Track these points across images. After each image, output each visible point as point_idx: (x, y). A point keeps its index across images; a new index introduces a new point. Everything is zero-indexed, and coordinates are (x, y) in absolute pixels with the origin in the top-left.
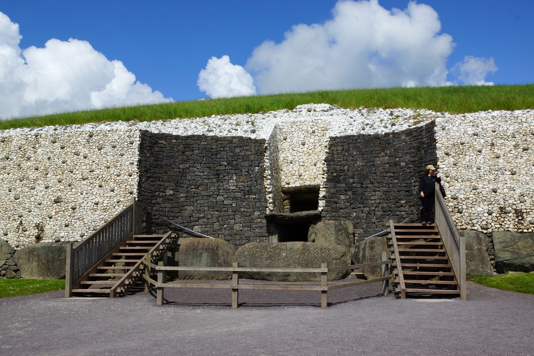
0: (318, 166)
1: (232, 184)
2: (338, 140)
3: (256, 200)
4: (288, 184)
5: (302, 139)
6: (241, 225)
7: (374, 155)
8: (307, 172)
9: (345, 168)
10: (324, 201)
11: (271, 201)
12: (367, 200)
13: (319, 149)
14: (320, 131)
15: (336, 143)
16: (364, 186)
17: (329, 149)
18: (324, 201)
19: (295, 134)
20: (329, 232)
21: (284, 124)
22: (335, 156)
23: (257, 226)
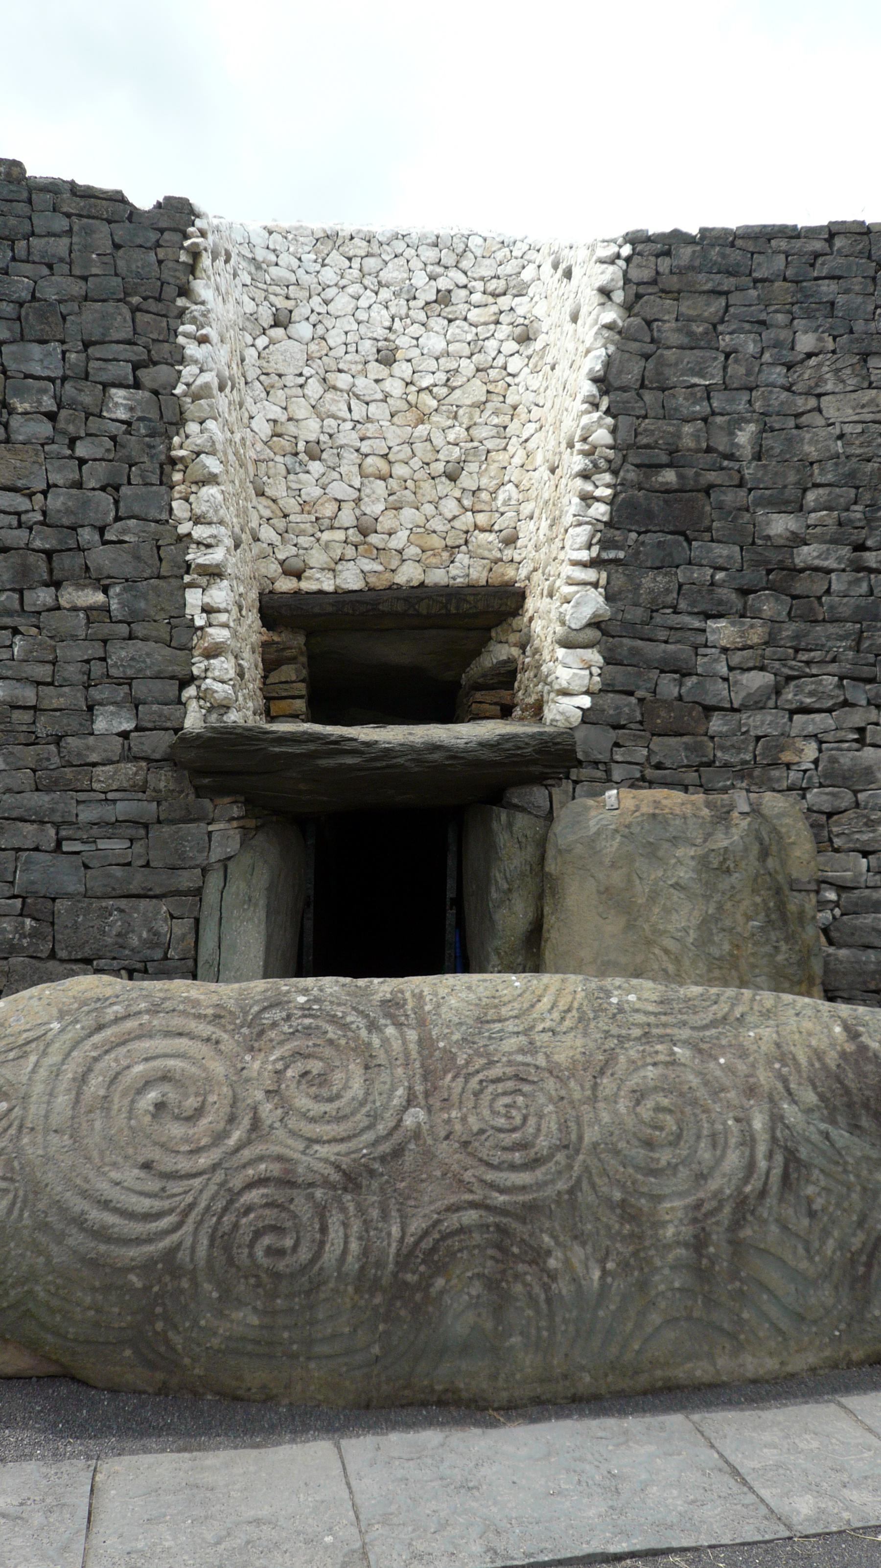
0: (466, 481)
3: (106, 629)
4: (298, 575)
5: (380, 333)
8: (408, 514)
11: (218, 634)
13: (477, 390)
14: (477, 298)
15: (678, 272)
17: (628, 308)
18: (594, 656)
19: (342, 303)
21: (276, 241)
22: (670, 355)
23: (110, 813)
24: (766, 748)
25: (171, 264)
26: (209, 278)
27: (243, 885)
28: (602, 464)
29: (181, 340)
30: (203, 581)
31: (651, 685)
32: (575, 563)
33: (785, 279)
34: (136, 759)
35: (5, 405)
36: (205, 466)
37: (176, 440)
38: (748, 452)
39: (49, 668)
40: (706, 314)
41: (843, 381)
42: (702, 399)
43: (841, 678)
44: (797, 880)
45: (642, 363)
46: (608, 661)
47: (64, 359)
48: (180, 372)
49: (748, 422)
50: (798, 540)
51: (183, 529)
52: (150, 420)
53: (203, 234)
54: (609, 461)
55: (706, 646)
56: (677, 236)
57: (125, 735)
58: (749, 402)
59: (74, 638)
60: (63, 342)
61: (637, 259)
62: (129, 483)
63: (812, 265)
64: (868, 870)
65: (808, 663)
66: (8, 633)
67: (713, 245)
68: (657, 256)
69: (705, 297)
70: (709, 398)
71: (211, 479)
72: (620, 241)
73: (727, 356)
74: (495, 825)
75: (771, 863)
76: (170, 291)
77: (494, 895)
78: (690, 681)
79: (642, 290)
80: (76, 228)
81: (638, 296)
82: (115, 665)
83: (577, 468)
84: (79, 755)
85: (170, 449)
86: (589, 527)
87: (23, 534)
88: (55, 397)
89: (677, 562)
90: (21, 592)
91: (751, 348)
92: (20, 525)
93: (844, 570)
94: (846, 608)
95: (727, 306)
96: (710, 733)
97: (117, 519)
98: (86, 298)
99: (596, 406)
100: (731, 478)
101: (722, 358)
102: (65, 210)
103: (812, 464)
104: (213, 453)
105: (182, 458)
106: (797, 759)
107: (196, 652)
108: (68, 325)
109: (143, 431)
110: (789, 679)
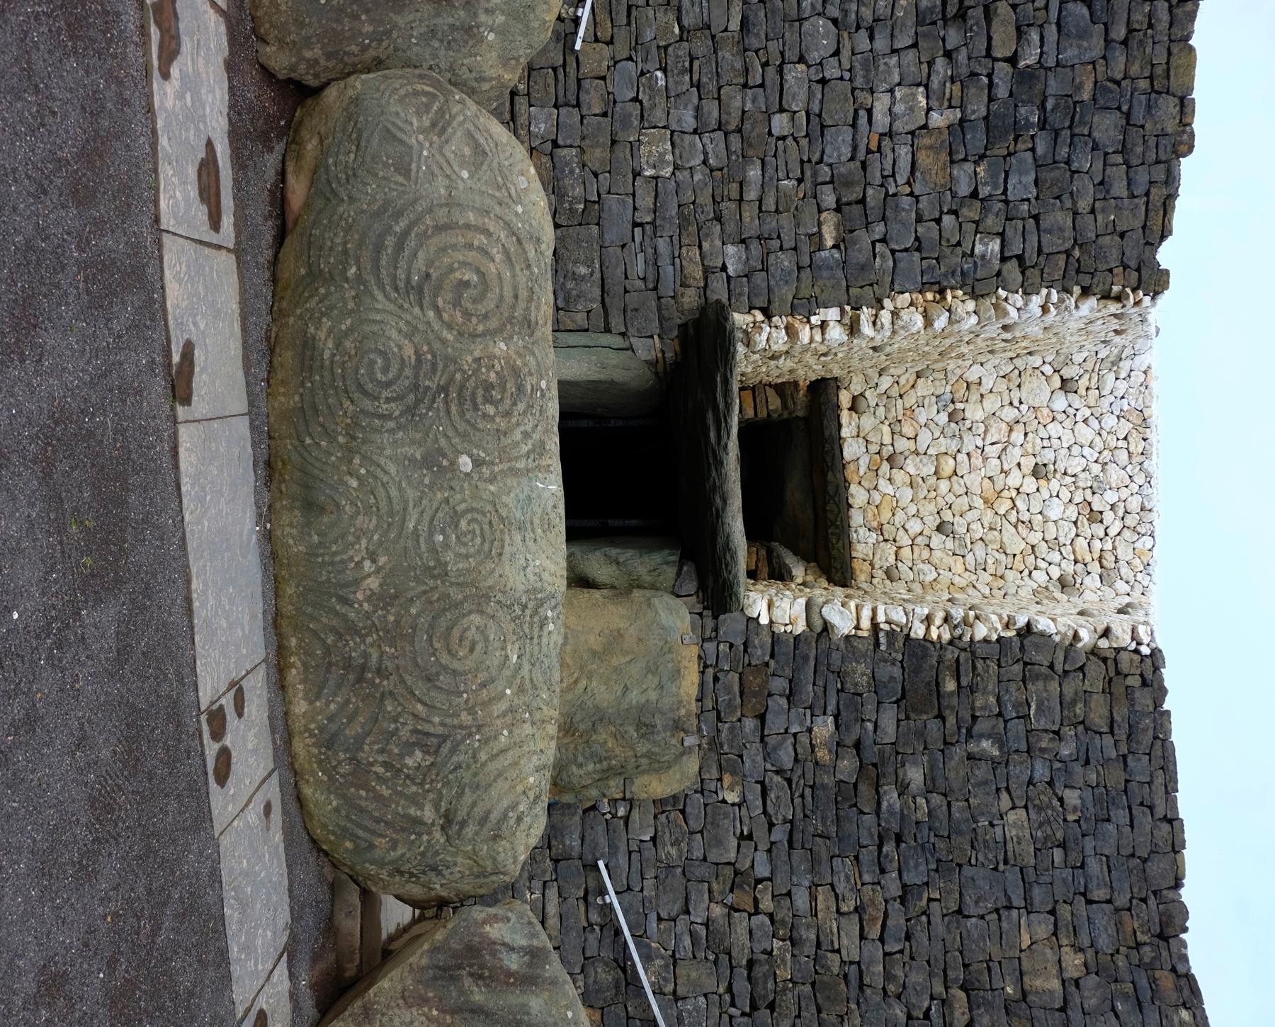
1: (897, 104)
2: (1144, 699)
3: (805, 248)
6: (667, 172)
7: (1064, 911)
9: (985, 744)
10: (800, 627)
11: (805, 334)
12: (812, 870)
14: (1097, 545)
16: (889, 848)
17: (1094, 652)
18: (800, 627)
20: (635, 670)
22: (1054, 686)
23: (665, 261)
24: (736, 761)
25: (1109, 280)
26: (1099, 311)
27: (614, 362)
28: (958, 632)
29: (1044, 291)
30: (847, 320)
31: (779, 673)
32: (874, 611)
33: (1127, 781)
34: (706, 279)
35: (982, 157)
36: (939, 317)
37: (960, 293)
38: (972, 747)
39: (773, 208)
40: (1092, 716)
41: (1040, 827)
42: (1017, 712)
43: (791, 822)
44: (632, 783)
45: (1046, 663)
46: (797, 638)
47: (1023, 200)
48: (1017, 292)
49: (1000, 750)
50: (903, 788)
51: (887, 302)
52: (975, 272)
53: (1137, 303)
54: (960, 638)
55: (812, 715)
56: (1163, 691)
57: (724, 268)
58: (1017, 751)
59: (797, 225)
60: (1037, 199)
61: (1136, 657)
62: (922, 259)
63: (1142, 804)
64: (641, 841)
65: (802, 796)
66: (799, 174)
67: (1154, 721)
68: (1141, 675)
69: (1108, 714)
70: (1018, 717)
71: (928, 323)
72: (1153, 645)
73: (1054, 732)
74: (666, 552)
75: (644, 761)
76: (1086, 280)
77: (614, 552)
78: (783, 702)
79: (1110, 662)
80: (1136, 200)
81: (1105, 660)
82: (777, 257)
83: (953, 612)
84: (708, 235)
85: (952, 288)
86: (904, 620)
87: (878, 181)
88: (990, 196)
89: (883, 692)
90: (832, 182)
91: (1066, 751)
92: (884, 177)
93: (879, 825)
94: (850, 828)
95: (1101, 733)
96: (744, 719)
97: (893, 252)
98: (1075, 213)
99: (1007, 626)
100: (951, 736)
101: (1056, 728)
102: (1153, 190)
103: (967, 800)
104: (951, 322)
105: (944, 298)
106: (726, 785)
107: (790, 318)
108: (1052, 201)
109: (966, 266)
110: (789, 781)
